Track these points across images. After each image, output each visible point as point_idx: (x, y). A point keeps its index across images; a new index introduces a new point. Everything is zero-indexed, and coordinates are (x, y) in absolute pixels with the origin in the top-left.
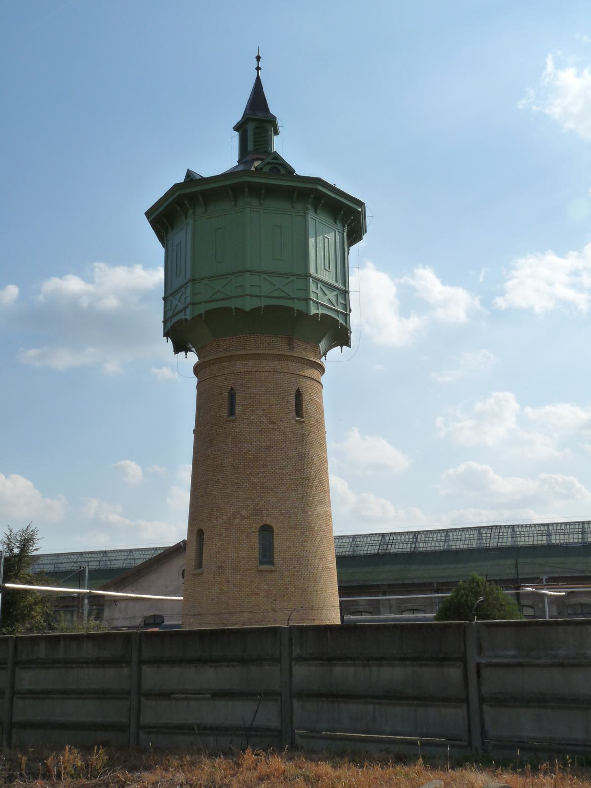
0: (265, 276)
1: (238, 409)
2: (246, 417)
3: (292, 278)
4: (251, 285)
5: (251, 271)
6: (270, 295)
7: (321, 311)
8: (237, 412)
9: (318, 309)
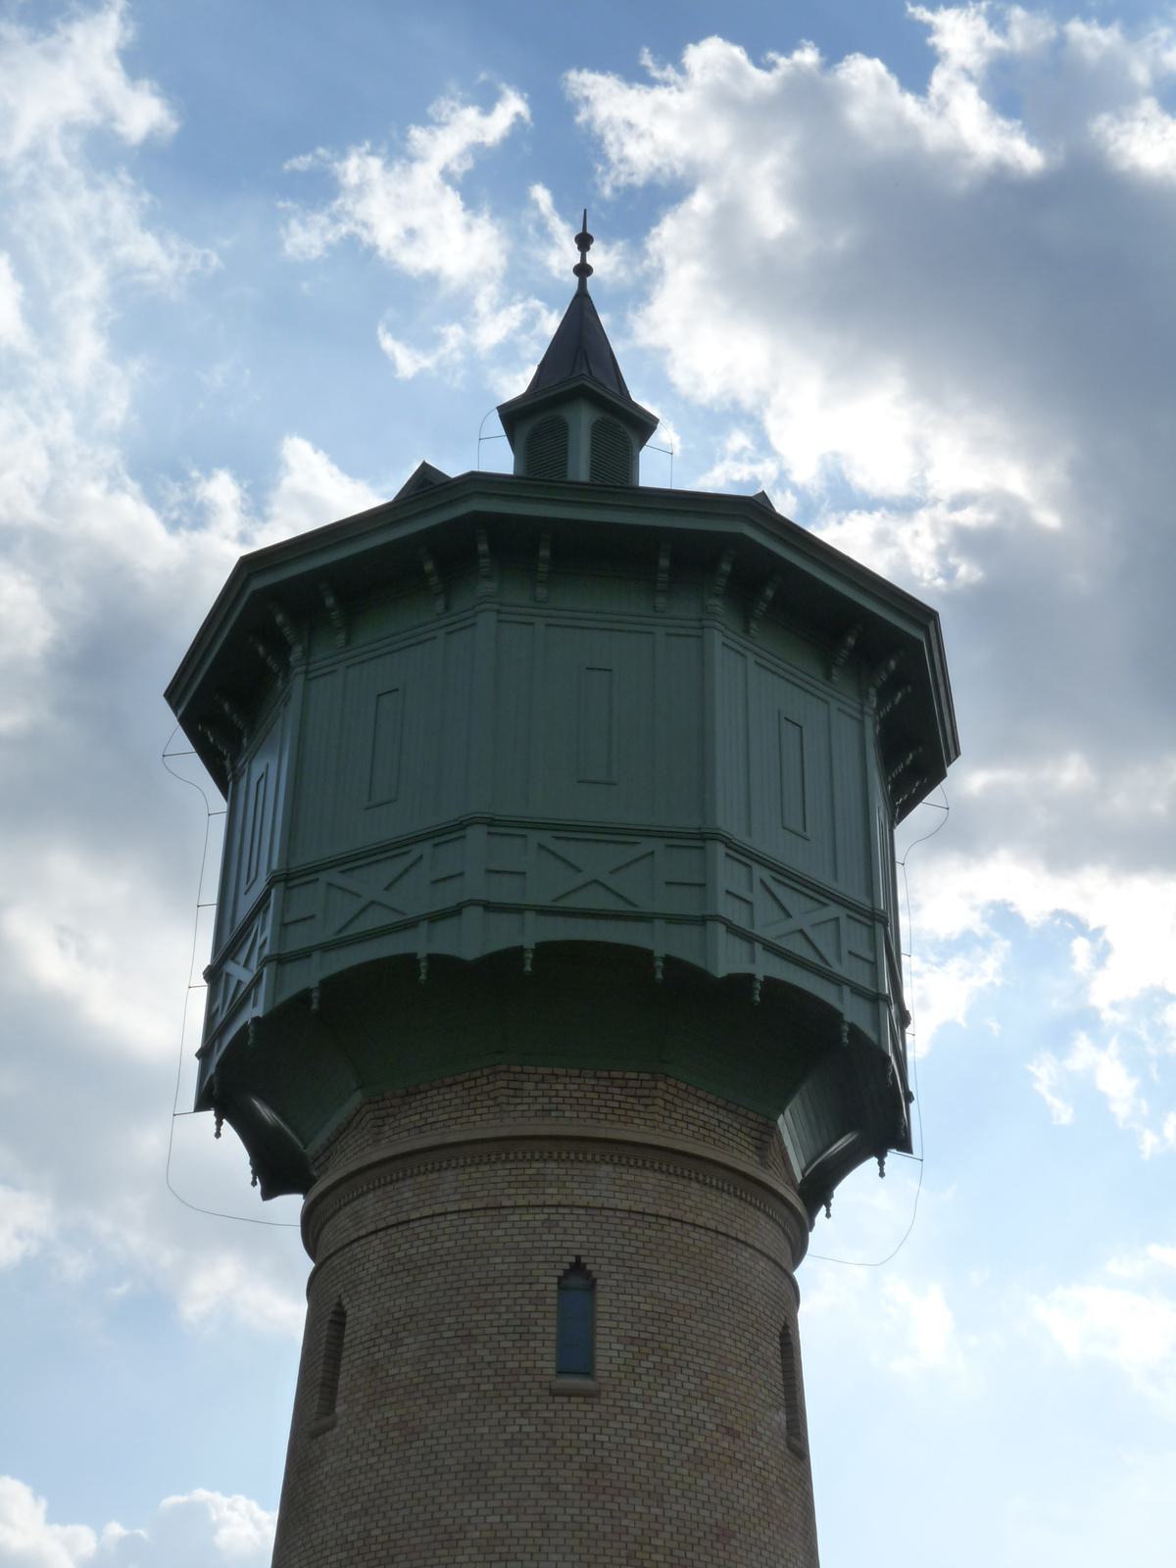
0: (546, 838)
1: (608, 1353)
2: (638, 1391)
3: (646, 845)
4: (489, 871)
5: (491, 822)
6: (559, 904)
7: (767, 967)
8: (601, 1363)
9: (753, 961)
